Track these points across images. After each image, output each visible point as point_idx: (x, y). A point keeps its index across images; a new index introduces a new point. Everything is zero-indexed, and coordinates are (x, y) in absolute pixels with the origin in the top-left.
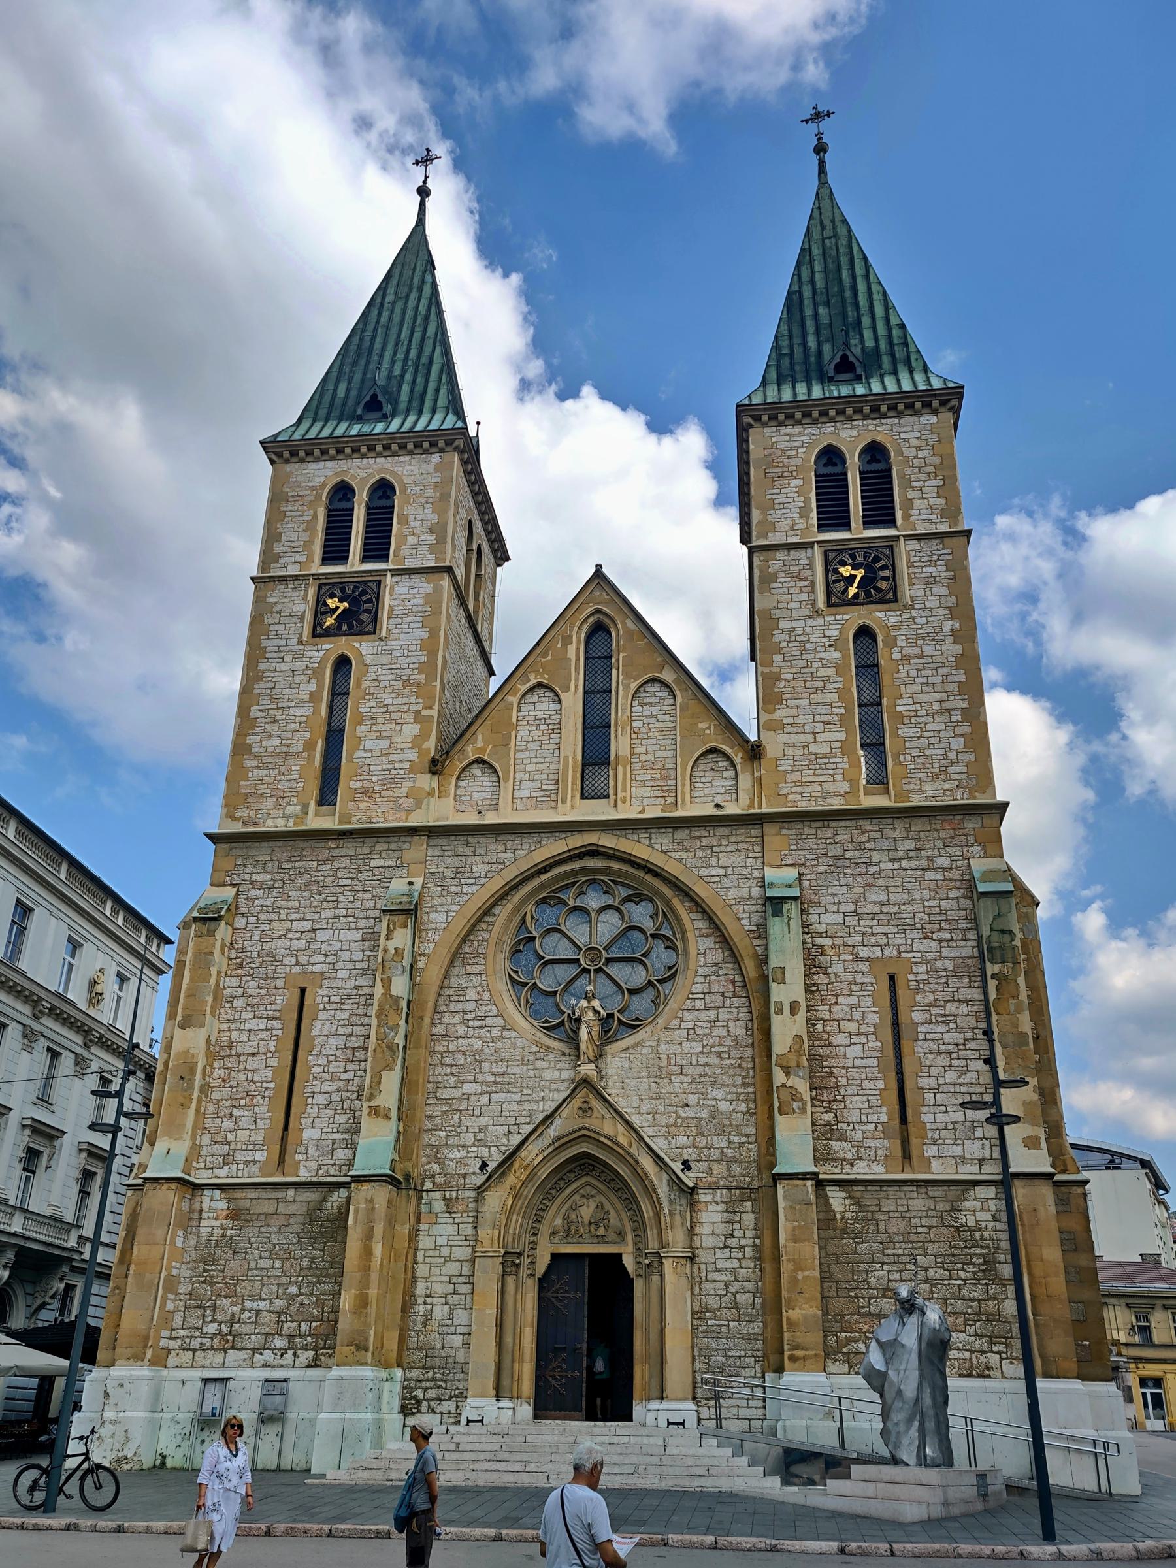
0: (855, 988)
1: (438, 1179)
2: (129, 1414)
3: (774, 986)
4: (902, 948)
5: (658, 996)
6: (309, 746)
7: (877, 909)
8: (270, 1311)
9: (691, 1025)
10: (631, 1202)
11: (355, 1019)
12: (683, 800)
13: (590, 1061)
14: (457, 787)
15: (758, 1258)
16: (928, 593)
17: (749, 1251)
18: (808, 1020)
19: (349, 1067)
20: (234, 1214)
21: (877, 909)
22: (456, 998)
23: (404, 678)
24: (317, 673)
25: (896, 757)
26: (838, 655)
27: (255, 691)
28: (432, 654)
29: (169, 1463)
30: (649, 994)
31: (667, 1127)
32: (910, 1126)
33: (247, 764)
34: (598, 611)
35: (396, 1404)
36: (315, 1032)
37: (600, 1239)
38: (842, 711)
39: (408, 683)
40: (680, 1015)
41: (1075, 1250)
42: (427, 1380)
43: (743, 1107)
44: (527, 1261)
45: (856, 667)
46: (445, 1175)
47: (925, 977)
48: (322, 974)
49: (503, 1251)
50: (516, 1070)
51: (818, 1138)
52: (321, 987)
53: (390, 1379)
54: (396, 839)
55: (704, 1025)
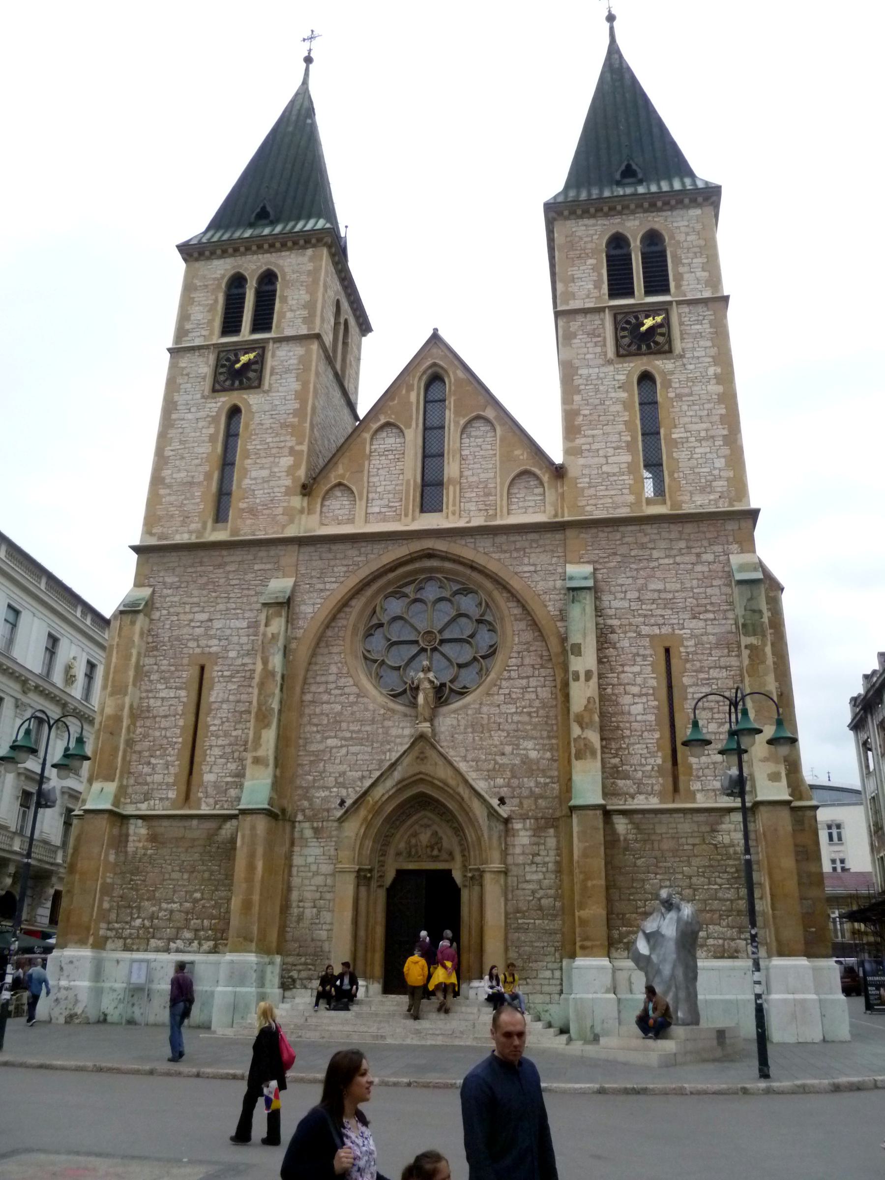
0: (638, 659)
1: (308, 812)
2: (77, 983)
3: (572, 658)
4: (676, 627)
5: (481, 669)
6: (208, 476)
7: (656, 595)
8: (180, 911)
9: (507, 691)
10: (458, 830)
11: (242, 690)
12: (501, 511)
13: (425, 720)
14: (322, 505)
15: (559, 871)
16: (696, 346)
17: (551, 866)
18: (600, 685)
19: (237, 727)
20: (153, 838)
21: (656, 595)
22: (322, 672)
23: (282, 421)
24: (215, 420)
25: (671, 475)
26: (625, 395)
27: (169, 436)
28: (303, 402)
29: (109, 1018)
30: (476, 667)
32: (680, 766)
33: (162, 492)
34: (435, 365)
35: (276, 981)
36: (212, 699)
37: (435, 859)
38: (629, 438)
39: (284, 425)
40: (498, 683)
41: (807, 859)
42: (301, 964)
43: (548, 755)
45: (640, 404)
46: (313, 810)
47: (694, 649)
48: (217, 653)
49: (357, 867)
50: (368, 728)
51: (607, 778)
52: (216, 664)
53: (271, 963)
54: (274, 548)
55: (518, 690)
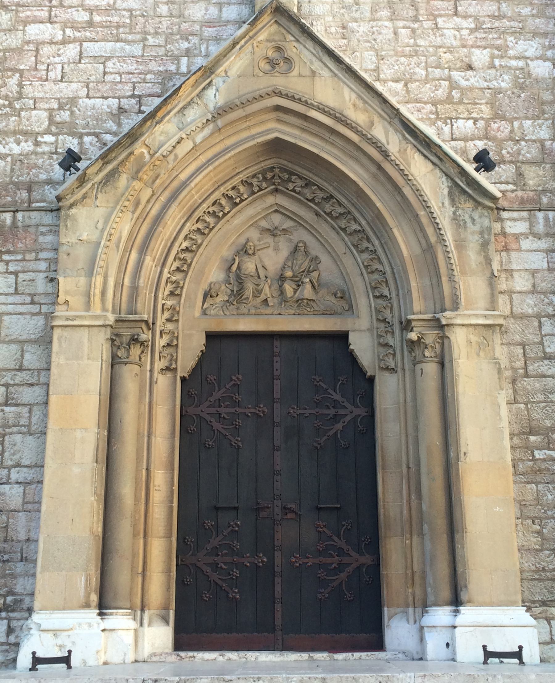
31: (434, 104)
44: (161, 342)
